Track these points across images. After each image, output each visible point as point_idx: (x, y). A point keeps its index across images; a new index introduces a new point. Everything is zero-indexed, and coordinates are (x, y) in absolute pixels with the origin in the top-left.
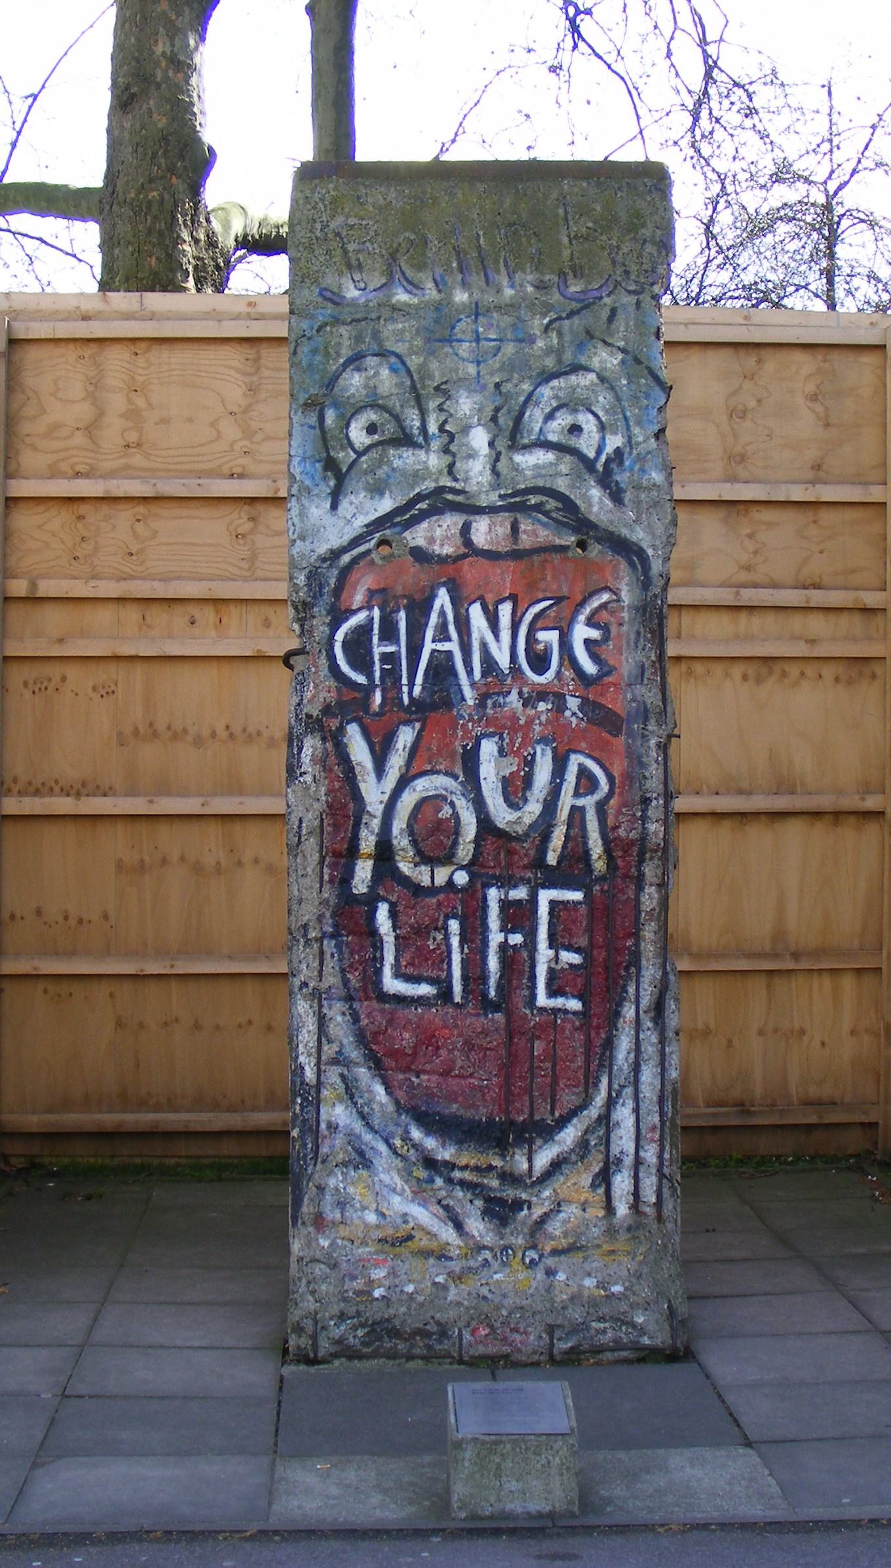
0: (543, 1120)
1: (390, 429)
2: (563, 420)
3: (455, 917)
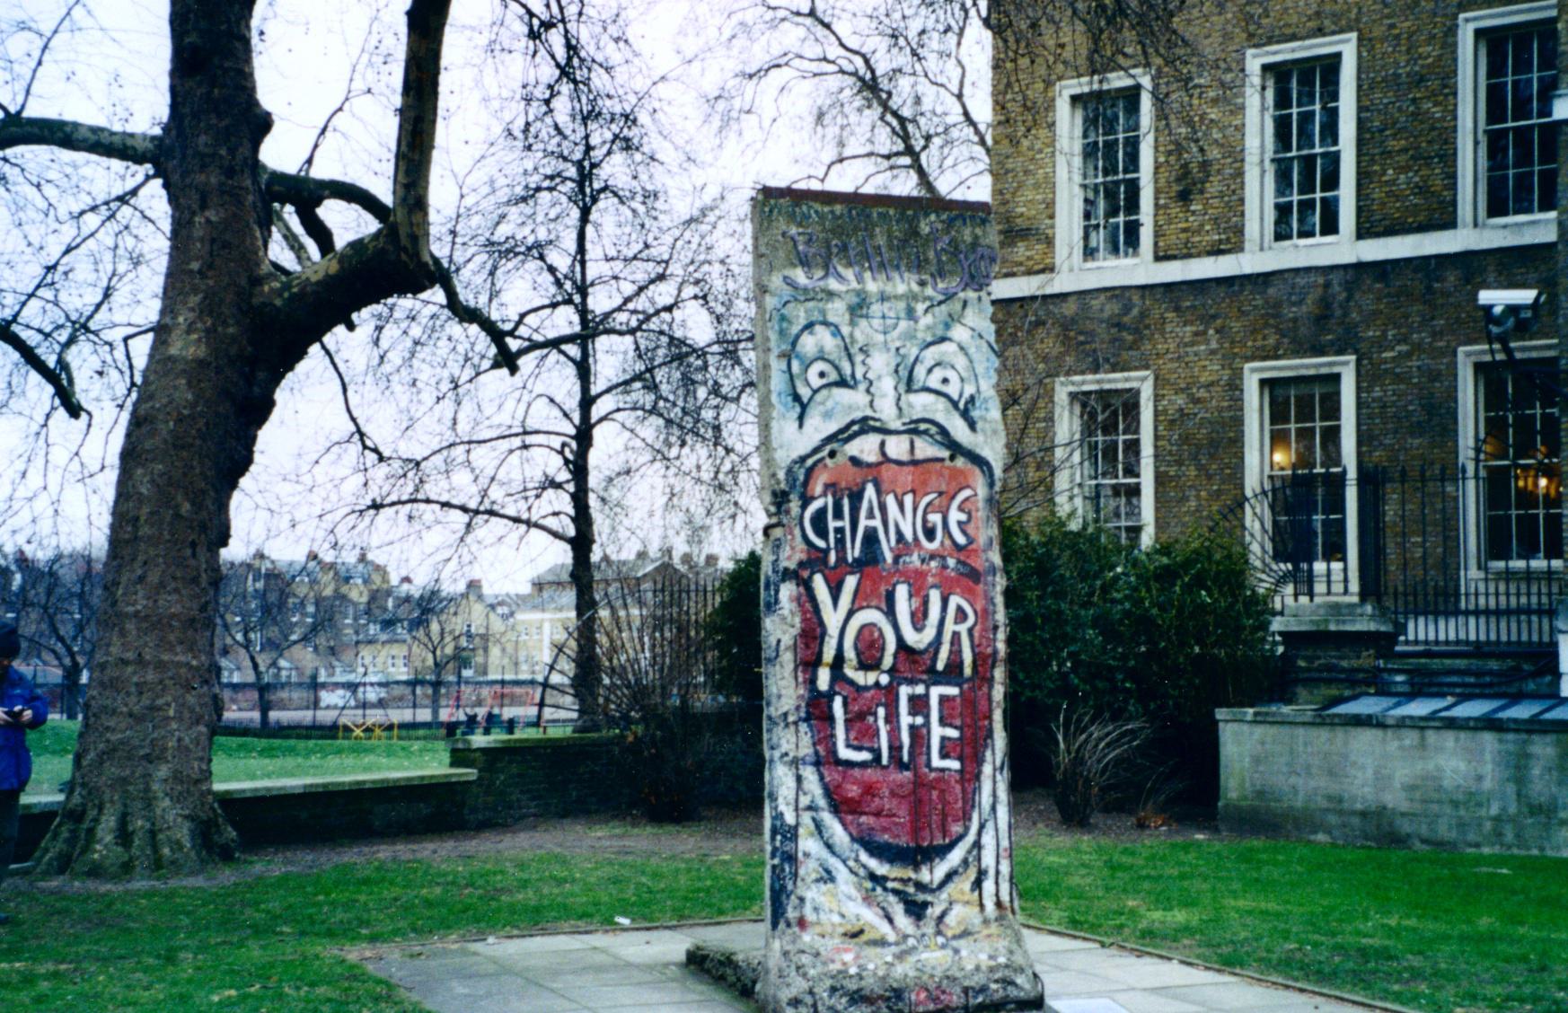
1: (833, 376)
2: (938, 374)
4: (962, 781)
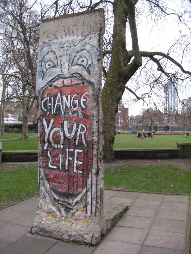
0: (75, 193)
1: (52, 65)
2: (81, 59)
3: (60, 154)
4: (83, 177)
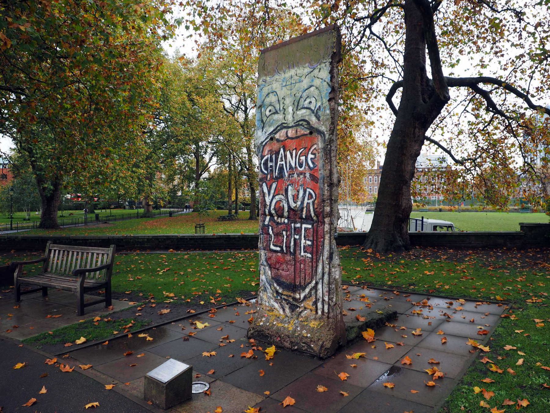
1: (274, 111)
2: (308, 101)
4: (312, 262)
